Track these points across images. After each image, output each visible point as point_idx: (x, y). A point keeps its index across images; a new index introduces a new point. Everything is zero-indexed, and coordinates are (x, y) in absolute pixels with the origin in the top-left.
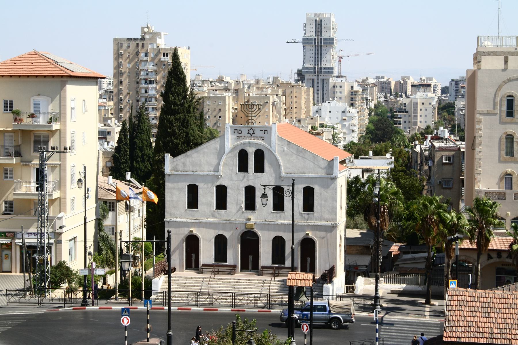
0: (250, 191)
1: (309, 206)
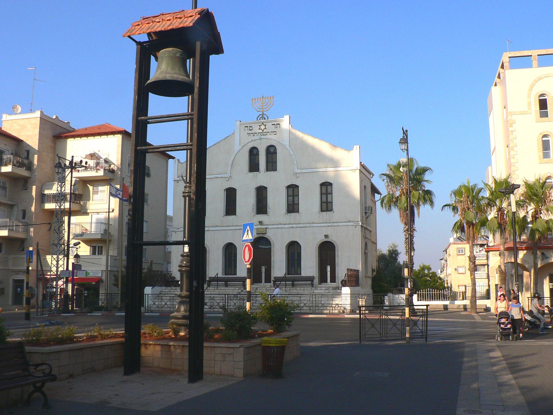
0: (261, 192)
1: (326, 206)
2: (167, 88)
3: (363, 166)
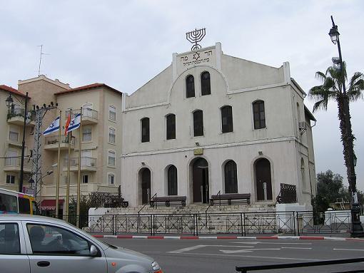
0: (198, 115)
1: (259, 122)
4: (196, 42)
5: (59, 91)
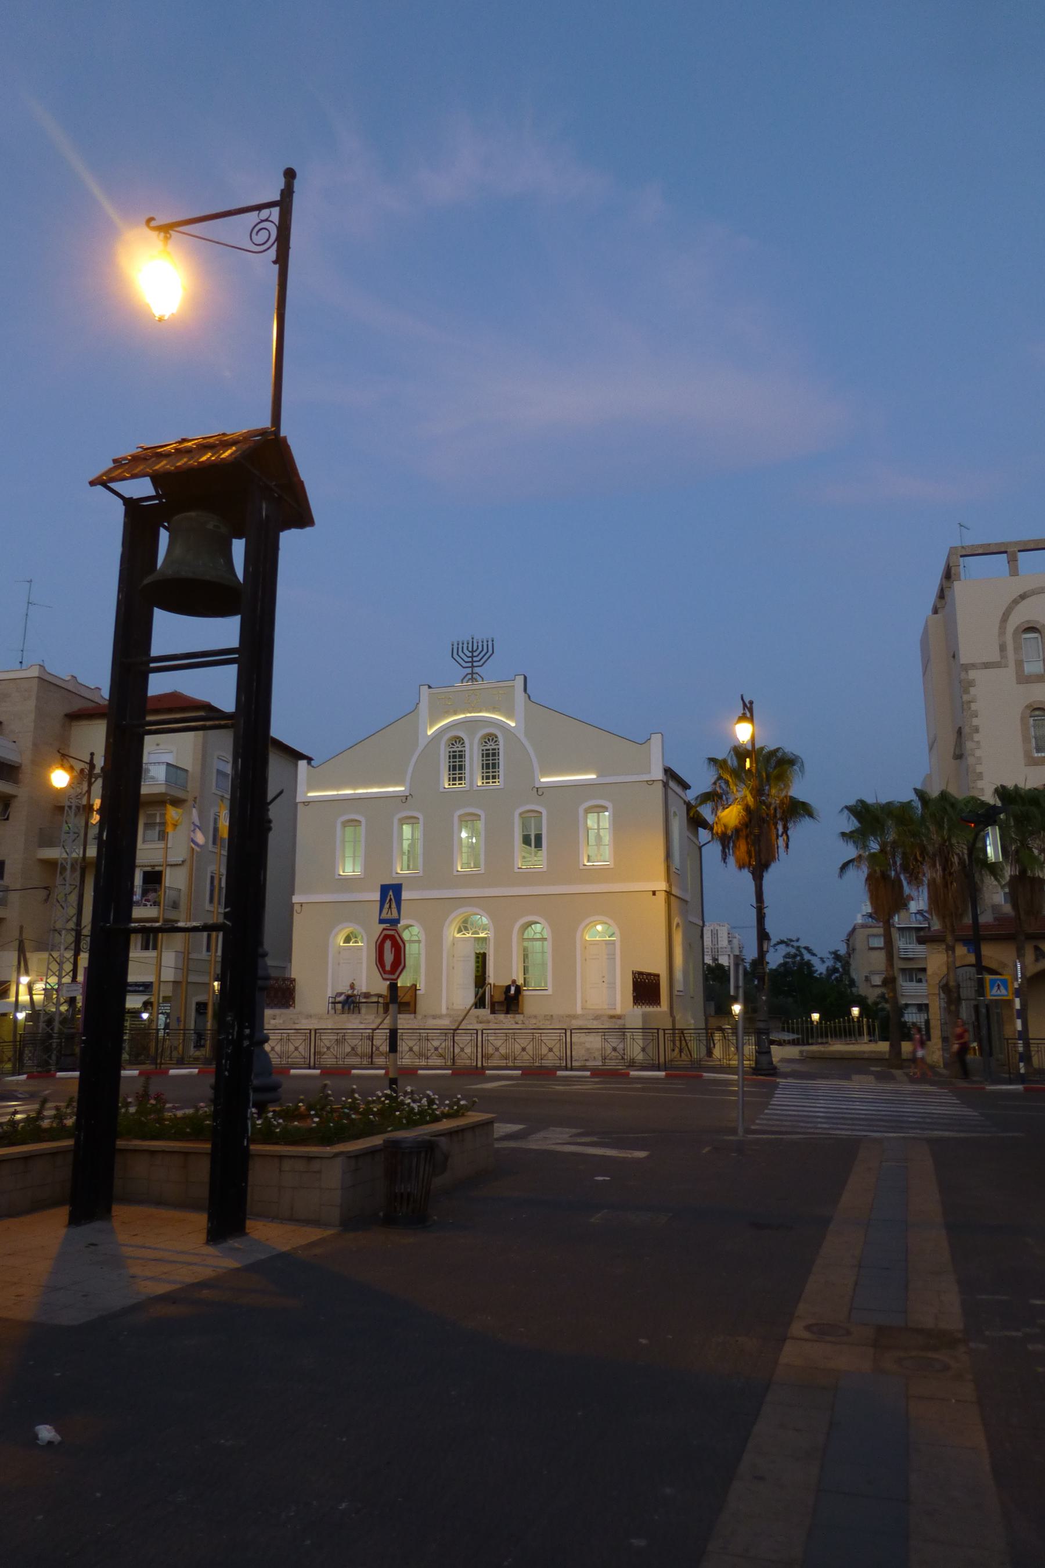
2: (199, 598)
3: (668, 772)
4: (473, 667)
5: (77, 705)
